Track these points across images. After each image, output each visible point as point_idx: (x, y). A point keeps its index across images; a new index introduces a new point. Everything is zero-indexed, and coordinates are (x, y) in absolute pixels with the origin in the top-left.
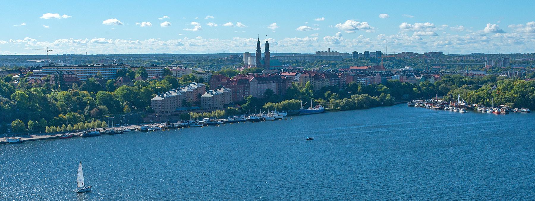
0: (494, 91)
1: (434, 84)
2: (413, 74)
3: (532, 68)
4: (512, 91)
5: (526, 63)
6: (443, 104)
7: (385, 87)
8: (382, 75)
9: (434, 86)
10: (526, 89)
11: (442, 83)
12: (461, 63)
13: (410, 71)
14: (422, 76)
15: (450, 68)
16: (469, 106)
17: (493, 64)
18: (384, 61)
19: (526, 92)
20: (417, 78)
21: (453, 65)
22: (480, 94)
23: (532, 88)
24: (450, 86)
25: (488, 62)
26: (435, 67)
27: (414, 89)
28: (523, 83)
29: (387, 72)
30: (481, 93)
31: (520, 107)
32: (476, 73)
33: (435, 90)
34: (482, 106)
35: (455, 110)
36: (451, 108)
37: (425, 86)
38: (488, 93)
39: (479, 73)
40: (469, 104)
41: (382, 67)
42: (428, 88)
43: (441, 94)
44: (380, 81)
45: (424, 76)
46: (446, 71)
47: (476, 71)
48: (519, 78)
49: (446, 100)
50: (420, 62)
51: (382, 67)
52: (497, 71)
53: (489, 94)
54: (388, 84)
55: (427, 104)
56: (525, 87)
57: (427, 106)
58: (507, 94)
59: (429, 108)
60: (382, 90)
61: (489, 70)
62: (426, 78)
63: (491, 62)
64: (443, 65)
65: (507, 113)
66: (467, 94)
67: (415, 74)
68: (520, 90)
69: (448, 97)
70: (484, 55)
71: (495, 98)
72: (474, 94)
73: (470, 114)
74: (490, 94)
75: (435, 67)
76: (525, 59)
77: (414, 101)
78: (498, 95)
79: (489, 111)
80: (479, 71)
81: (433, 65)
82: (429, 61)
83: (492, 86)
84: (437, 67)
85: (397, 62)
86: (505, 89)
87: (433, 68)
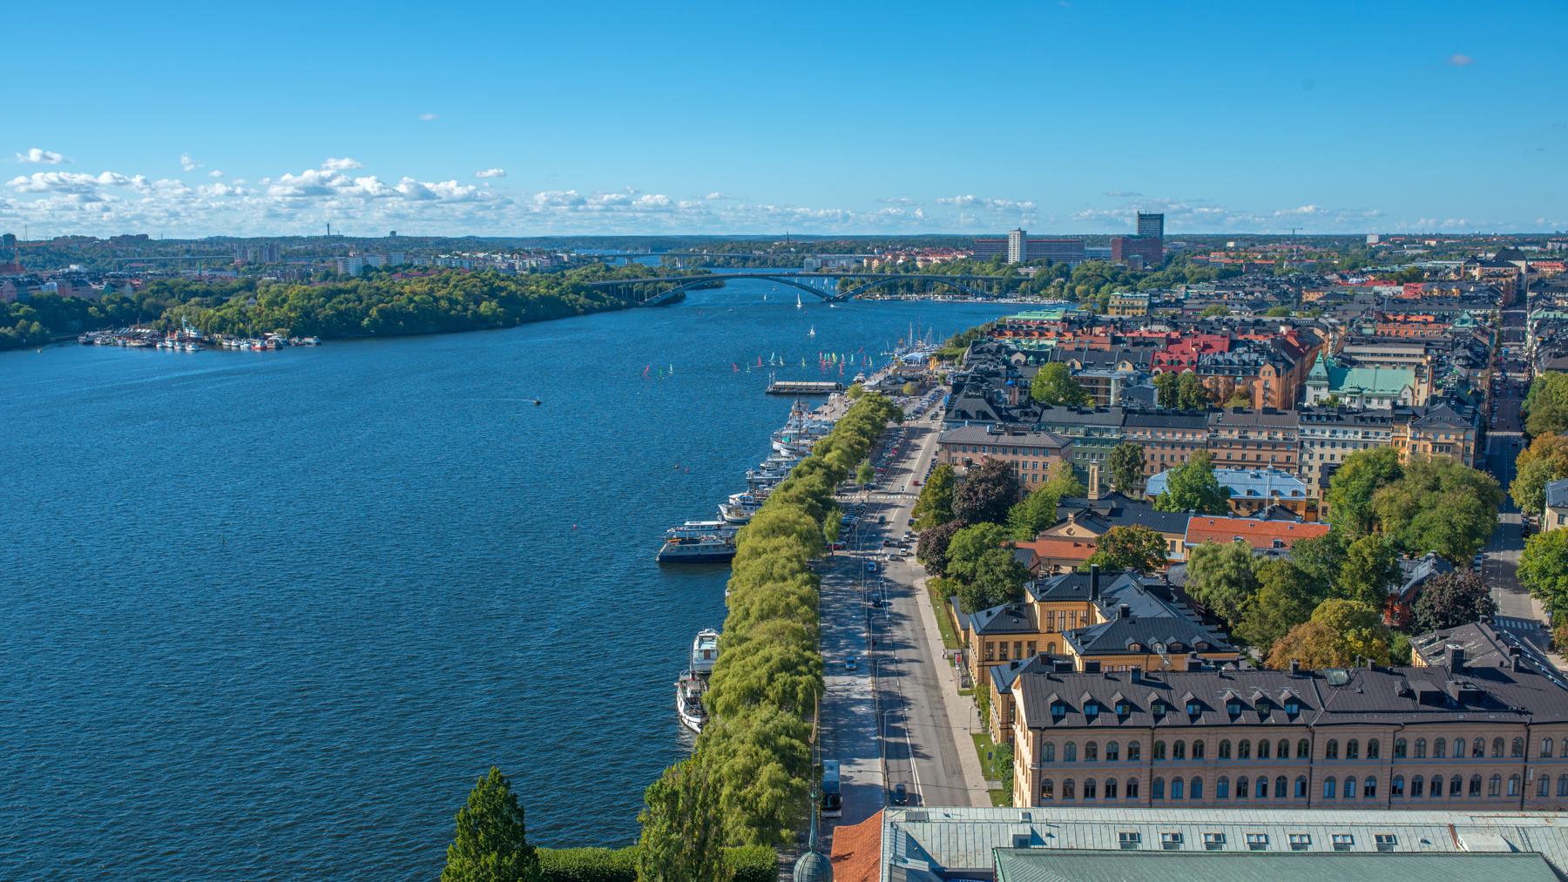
0: (251, 308)
1: (133, 299)
2: (86, 279)
3: (323, 262)
4: (286, 306)
5: (311, 254)
6: (153, 336)
7: (26, 307)
8: (17, 283)
9: (132, 303)
10: (312, 302)
11: (148, 296)
12: (188, 257)
13: (80, 273)
14: (105, 283)
15: (164, 265)
16: (206, 339)
17: (250, 257)
18: (23, 255)
19: (312, 306)
20: (94, 287)
21: (172, 260)
22: (225, 314)
23: (322, 299)
24: (166, 300)
25: (239, 253)
26: (134, 265)
27: (90, 310)
28: (305, 290)
29: (30, 276)
30: (228, 312)
31: (302, 336)
32: (218, 274)
33: (134, 310)
34: (231, 336)
35: (178, 348)
36: (169, 344)
37: (113, 302)
38: (240, 312)
39: (223, 274)
40: (206, 334)
41: (18, 267)
42: (120, 308)
43: (148, 317)
44: (14, 296)
45: (109, 284)
46: (158, 272)
47: (217, 270)
48: (299, 282)
49: (159, 329)
50: (103, 256)
51: (18, 267)
52: (257, 269)
53: (243, 315)
54: (33, 302)
55: (119, 338)
56: (309, 297)
57: (120, 342)
58: (276, 312)
59: (125, 346)
60: (21, 312)
61: (243, 269)
62: (114, 286)
63: (245, 253)
64: (150, 261)
65: (279, 347)
66: (199, 316)
67: (90, 280)
68: (300, 304)
69: (162, 322)
70: (232, 240)
71: (254, 321)
72: (214, 315)
73: (208, 354)
74: (245, 315)
75: (134, 265)
76: (310, 247)
77: (91, 334)
78: (259, 315)
79: (244, 346)
80: (220, 270)
81: (131, 261)
82: (122, 254)
83: (248, 298)
84: (138, 265)
85: (53, 257)
86: (272, 304)
87: (131, 268)
